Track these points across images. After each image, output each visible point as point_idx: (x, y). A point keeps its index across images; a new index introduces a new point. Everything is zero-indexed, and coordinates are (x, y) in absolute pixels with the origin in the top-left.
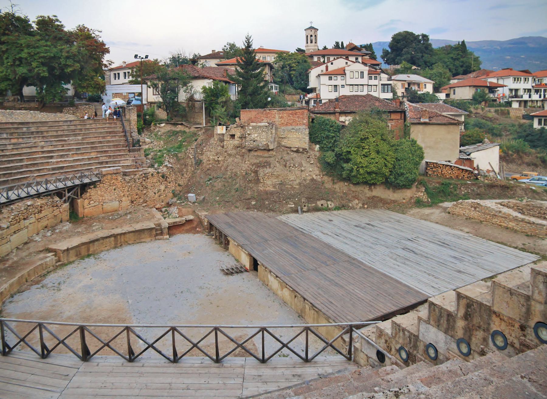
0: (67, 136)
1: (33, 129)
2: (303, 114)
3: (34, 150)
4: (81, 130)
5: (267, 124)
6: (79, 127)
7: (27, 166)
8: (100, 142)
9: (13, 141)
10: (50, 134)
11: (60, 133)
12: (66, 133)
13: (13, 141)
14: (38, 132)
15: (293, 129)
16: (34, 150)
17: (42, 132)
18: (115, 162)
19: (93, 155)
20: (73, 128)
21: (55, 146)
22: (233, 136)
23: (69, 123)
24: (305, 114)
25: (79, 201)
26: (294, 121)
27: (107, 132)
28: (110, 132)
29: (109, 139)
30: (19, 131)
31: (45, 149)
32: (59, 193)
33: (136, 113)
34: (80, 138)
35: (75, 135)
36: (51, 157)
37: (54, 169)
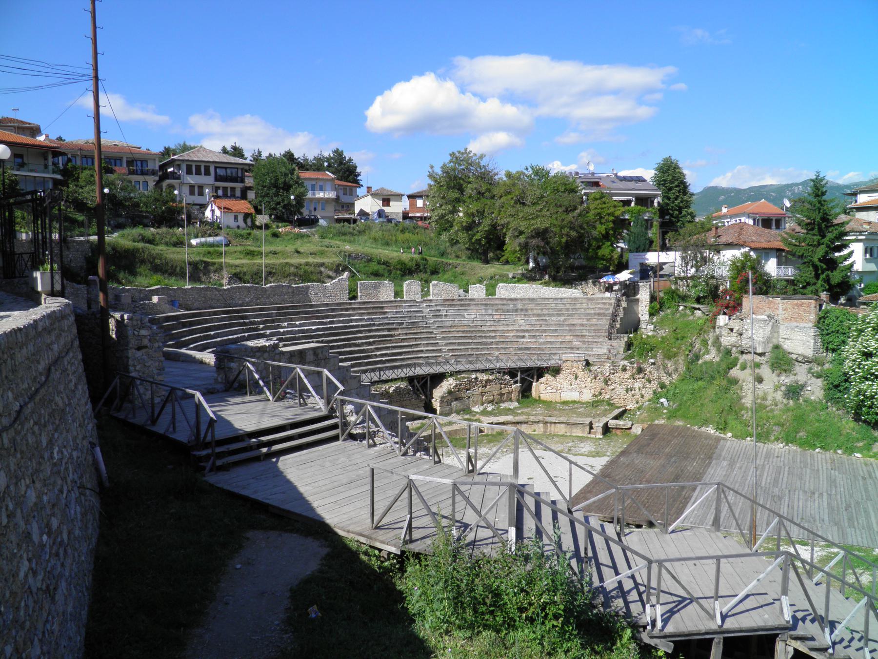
0: (550, 315)
1: (520, 306)
2: (809, 306)
3: (511, 328)
4: (567, 310)
5: (765, 317)
6: (568, 306)
7: (497, 343)
8: (582, 325)
9: (495, 317)
10: (535, 312)
11: (545, 312)
12: (551, 312)
13: (495, 317)
14: (522, 310)
15: (797, 327)
16: (511, 328)
17: (526, 310)
18: (587, 349)
19: (568, 338)
20: (561, 306)
21: (533, 325)
22: (732, 330)
23: (559, 302)
24: (813, 306)
25: (534, 384)
26: (800, 316)
27: (595, 314)
28: (599, 314)
29: (594, 321)
30: (505, 307)
31: (522, 328)
32: (512, 373)
33: (648, 290)
34: (562, 318)
35: (559, 315)
36: (524, 337)
37: (520, 349)
